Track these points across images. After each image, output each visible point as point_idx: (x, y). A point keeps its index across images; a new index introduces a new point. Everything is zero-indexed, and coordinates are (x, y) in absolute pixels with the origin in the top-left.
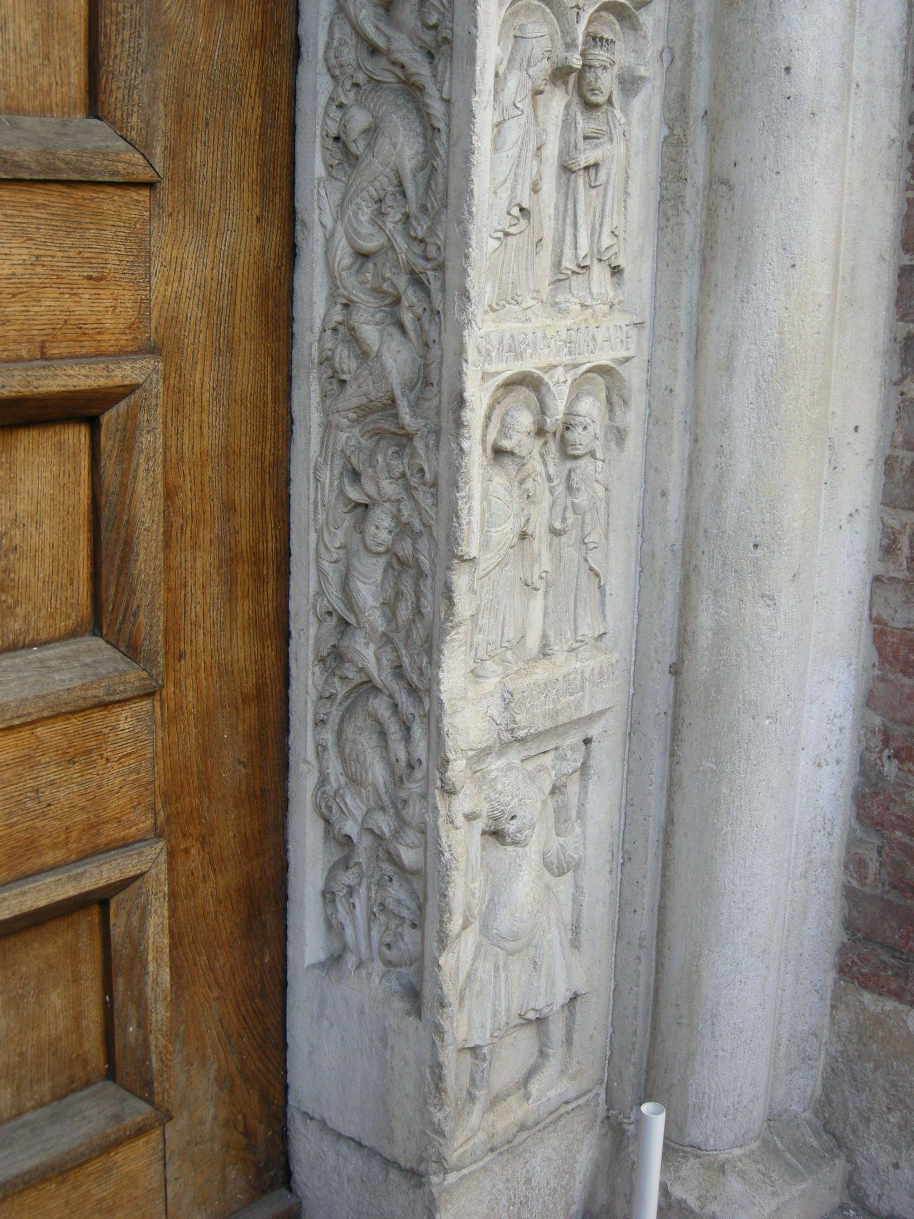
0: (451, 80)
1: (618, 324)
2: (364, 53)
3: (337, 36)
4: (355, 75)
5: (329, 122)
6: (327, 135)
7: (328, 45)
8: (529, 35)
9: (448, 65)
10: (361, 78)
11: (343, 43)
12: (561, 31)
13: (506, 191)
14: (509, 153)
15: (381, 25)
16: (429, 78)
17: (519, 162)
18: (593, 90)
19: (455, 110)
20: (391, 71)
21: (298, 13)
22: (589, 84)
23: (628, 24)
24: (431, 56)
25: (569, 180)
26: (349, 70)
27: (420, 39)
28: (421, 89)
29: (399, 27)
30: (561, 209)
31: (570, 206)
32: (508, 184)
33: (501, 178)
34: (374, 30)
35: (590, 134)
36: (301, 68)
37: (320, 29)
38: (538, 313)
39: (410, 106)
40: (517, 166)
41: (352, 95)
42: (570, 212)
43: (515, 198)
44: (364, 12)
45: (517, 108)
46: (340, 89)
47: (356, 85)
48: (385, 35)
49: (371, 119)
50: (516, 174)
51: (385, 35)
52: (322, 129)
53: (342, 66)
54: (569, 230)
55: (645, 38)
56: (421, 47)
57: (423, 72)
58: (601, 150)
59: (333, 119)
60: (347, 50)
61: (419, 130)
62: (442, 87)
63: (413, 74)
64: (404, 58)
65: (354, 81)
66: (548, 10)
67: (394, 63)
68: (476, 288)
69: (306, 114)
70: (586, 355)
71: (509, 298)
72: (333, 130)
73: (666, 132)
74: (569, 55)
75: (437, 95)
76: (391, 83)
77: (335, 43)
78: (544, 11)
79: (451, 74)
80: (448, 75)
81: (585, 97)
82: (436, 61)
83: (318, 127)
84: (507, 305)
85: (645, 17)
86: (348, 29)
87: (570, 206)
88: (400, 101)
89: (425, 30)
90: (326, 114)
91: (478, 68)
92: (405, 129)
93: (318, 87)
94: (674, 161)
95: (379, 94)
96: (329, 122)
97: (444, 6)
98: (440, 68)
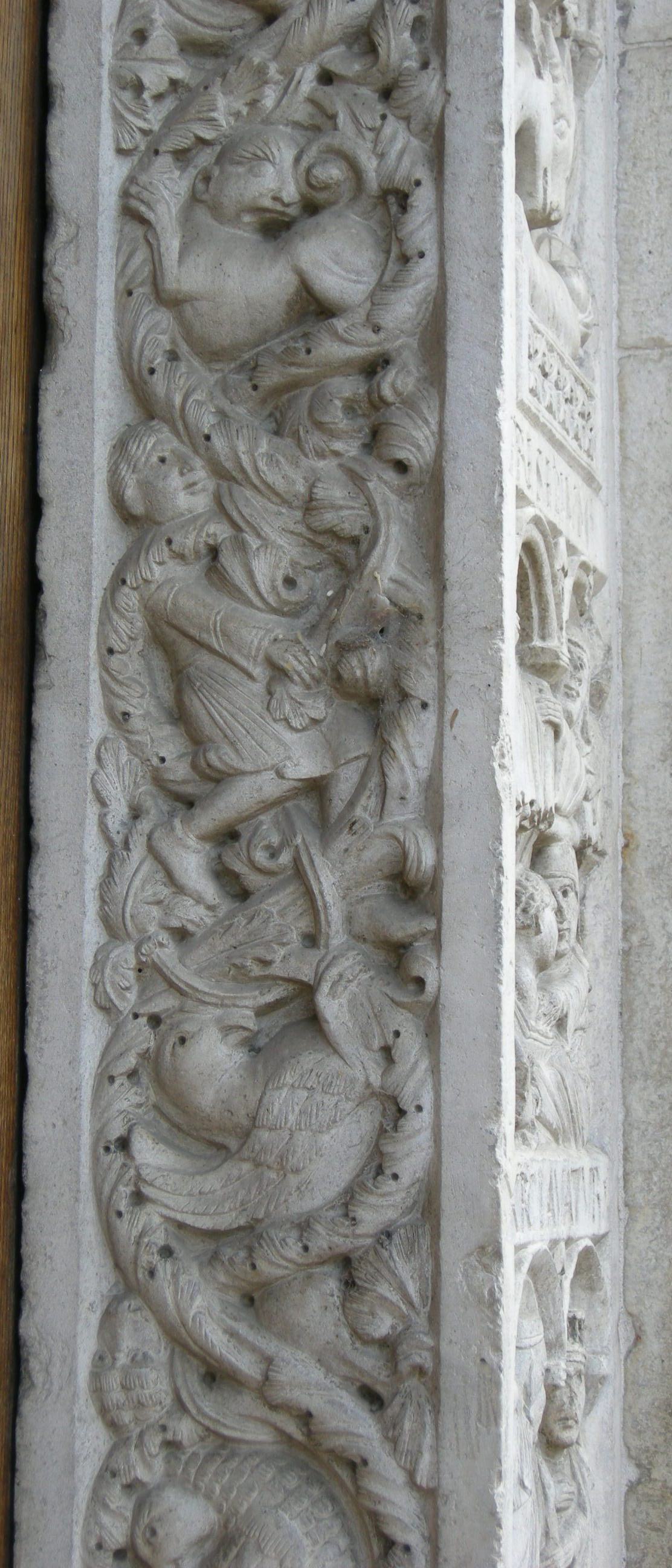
0: (436, 1449)
2: (192, 1385)
3: (127, 1343)
4: (171, 1425)
5: (106, 1519)
6: (100, 1546)
7: (102, 1361)
9: (428, 1419)
10: (185, 1430)
11: (139, 1360)
15: (243, 1329)
16: (376, 1444)
18: (567, 1419)
19: (449, 1511)
20: (265, 1422)
21: (19, 1292)
22: (560, 1409)
23: (584, 1282)
24: (372, 1398)
26: (154, 1414)
27: (345, 1360)
28: (356, 1466)
29: (289, 1335)
34: (225, 1338)
36: (27, 1406)
37: (80, 1326)
39: (316, 1492)
41: (159, 1465)
44: (198, 1301)
46: (134, 1454)
47: (172, 1446)
48: (254, 1349)
49: (213, 1515)
51: (254, 1349)
52: (87, 1533)
53: (140, 1405)
55: (603, 1303)
56: (346, 1378)
57: (361, 1431)
59: (116, 1514)
60: (153, 1375)
61: (343, 1542)
62: (416, 1462)
63: (337, 1433)
64: (314, 1402)
65: (169, 1436)
67: (274, 1407)
69: (44, 1501)
72: (117, 1533)
73: (633, 1473)
74: (552, 1363)
75: (400, 1477)
76: (260, 1443)
77: (123, 1359)
79: (437, 1437)
80: (428, 1440)
81: (551, 1433)
82: (392, 1410)
83: (78, 1530)
86: (152, 1331)
88: (292, 1481)
89: (358, 1345)
90: (97, 1499)
91: (503, 1430)
92: (315, 1543)
93: (78, 1443)
94: (657, 1530)
95: (234, 1464)
96: (106, 1519)
97: (410, 1303)
98: (407, 1425)
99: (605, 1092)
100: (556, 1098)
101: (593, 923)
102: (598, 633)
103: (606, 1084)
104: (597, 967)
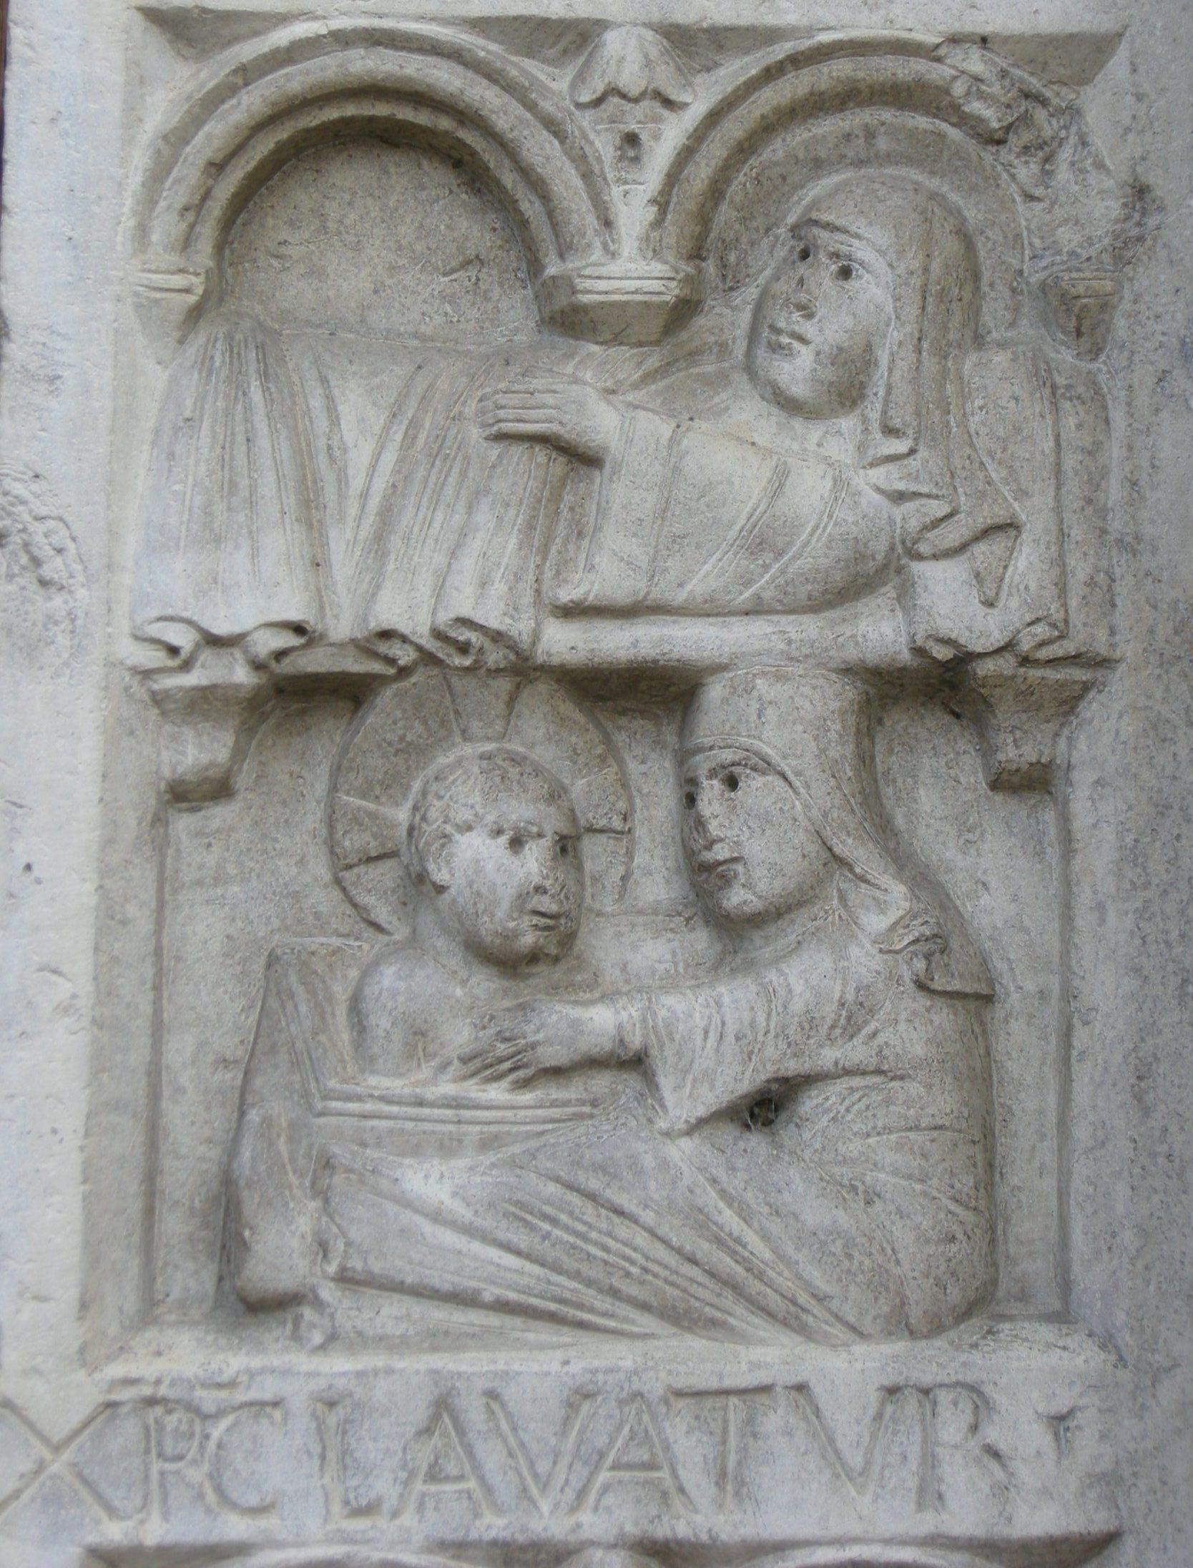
99: (1120, 1209)
100: (521, 1239)
101: (1090, 821)
102: (1100, 166)
103: (1122, 1189)
104: (1102, 921)
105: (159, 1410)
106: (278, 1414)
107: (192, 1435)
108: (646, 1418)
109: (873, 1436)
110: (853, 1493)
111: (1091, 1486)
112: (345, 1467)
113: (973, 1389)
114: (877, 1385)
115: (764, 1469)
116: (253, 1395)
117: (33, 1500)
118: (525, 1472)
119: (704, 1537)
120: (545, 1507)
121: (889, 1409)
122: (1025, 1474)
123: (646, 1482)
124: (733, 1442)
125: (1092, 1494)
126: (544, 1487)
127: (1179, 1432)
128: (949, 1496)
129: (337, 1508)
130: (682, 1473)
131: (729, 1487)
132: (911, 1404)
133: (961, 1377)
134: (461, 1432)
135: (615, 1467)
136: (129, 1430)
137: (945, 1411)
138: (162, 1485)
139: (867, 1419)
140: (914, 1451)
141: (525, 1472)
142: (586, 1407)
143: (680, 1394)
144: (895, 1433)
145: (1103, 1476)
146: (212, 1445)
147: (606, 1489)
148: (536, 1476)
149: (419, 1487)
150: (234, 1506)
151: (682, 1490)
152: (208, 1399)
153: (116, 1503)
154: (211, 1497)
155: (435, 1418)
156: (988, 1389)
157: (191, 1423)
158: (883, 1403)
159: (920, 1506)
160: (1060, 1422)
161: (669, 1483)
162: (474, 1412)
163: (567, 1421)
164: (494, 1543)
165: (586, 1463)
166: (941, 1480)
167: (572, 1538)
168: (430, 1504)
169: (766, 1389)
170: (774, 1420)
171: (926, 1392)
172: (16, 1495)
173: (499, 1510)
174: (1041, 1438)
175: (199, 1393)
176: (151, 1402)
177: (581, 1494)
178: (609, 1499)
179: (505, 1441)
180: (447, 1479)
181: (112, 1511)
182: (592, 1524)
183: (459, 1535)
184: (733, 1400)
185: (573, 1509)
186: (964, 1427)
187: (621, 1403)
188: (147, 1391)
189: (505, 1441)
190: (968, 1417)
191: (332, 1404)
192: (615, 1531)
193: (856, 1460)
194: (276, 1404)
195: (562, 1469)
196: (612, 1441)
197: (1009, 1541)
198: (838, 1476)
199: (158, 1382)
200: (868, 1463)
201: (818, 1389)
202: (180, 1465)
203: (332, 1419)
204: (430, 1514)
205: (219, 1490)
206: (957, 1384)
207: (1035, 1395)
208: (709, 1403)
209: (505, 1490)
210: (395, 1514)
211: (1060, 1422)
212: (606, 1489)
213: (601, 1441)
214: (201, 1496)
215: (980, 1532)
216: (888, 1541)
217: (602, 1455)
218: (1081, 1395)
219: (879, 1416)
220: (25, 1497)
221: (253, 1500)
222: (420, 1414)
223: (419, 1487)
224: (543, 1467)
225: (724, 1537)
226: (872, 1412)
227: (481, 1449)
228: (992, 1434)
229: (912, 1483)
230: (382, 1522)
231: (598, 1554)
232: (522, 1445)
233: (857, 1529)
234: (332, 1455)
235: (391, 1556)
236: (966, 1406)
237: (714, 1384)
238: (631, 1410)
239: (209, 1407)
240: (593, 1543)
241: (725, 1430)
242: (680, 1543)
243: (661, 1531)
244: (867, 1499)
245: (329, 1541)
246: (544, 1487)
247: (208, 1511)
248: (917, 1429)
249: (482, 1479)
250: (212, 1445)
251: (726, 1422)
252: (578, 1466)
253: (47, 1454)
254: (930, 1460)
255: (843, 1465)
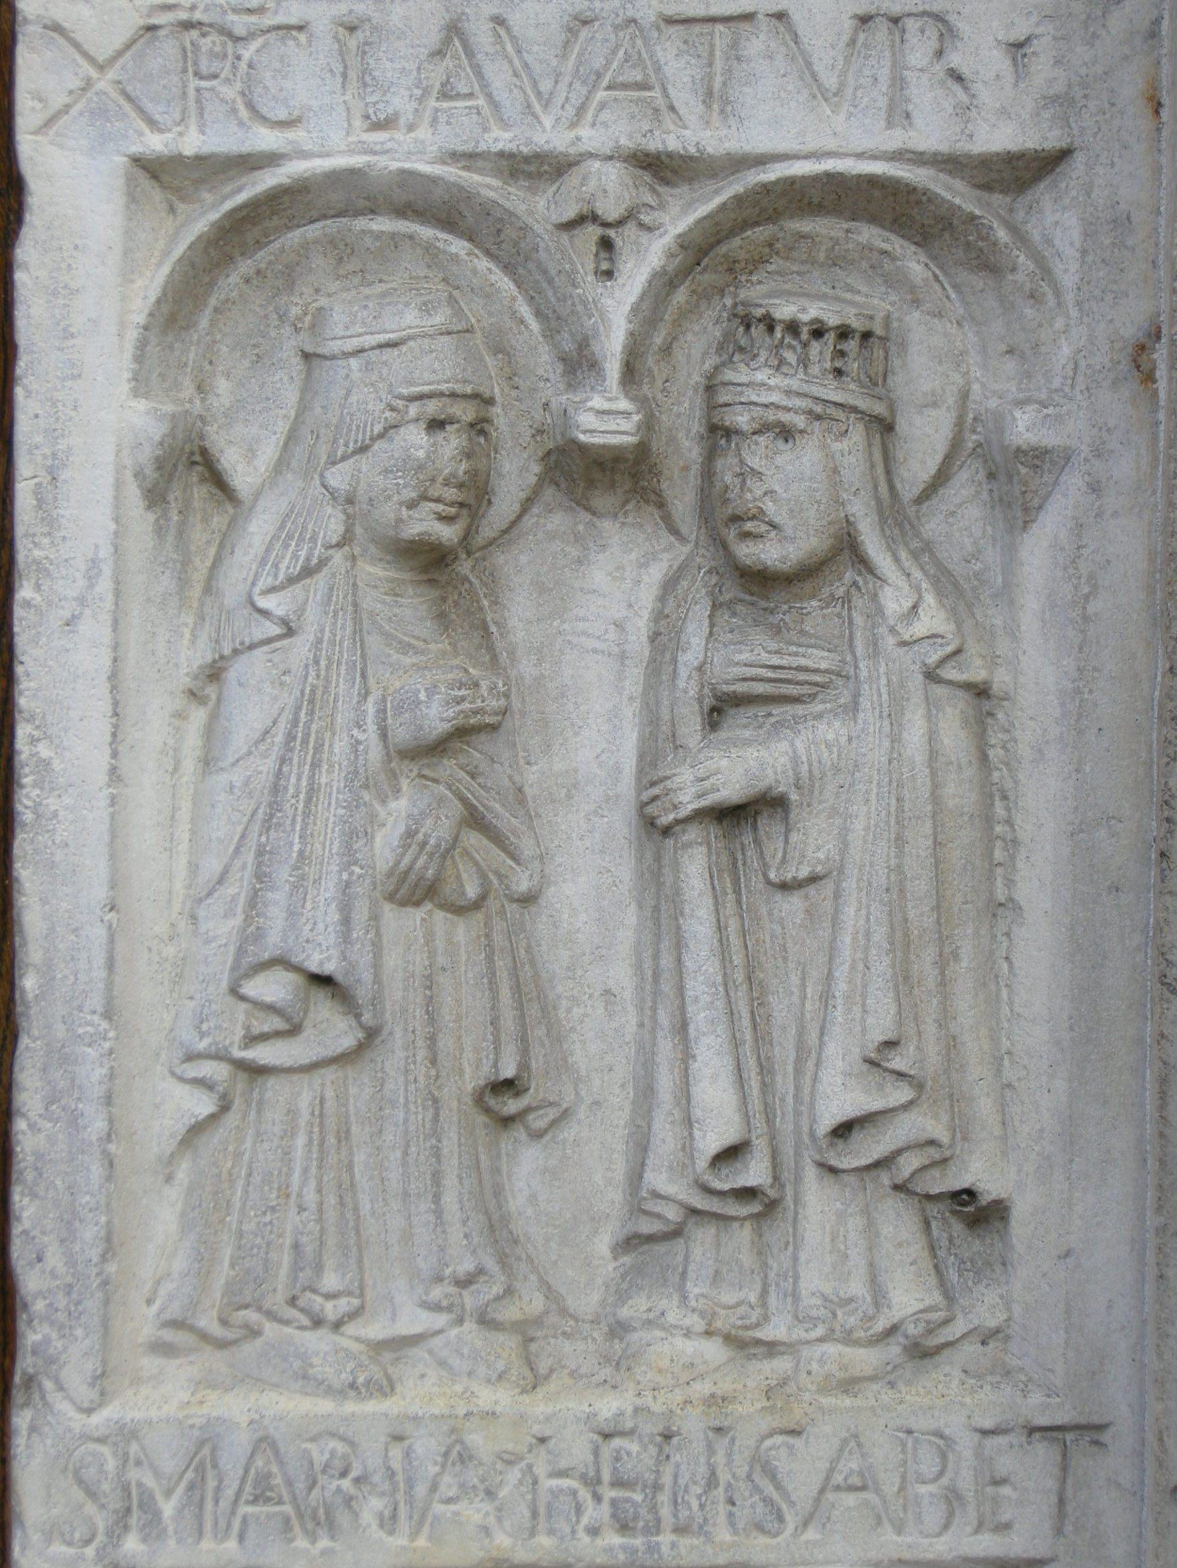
1: (922, 1423)
8: (335, 346)
12: (538, 314)
13: (229, 913)
14: (237, 777)
17: (275, 806)
23: (960, 253)
25: (658, 858)
30: (648, 965)
31: (667, 961)
32: (237, 888)
33: (212, 866)
35: (741, 688)
38: (455, 1362)
40: (268, 825)
42: (667, 987)
43: (259, 936)
45: (264, 613)
50: (261, 852)
54: (666, 1047)
58: (784, 746)
66: (458, 246)
68: (55, 1259)
70: (724, 1535)
71: (277, 1300)
78: (430, 251)
84: (270, 1328)
85: (1050, 217)
87: (667, 961)
105: (194, 33)
106: (303, 37)
107: (225, 55)
108: (639, 42)
109: (848, 59)
110: (829, 112)
111: (1045, 107)
112: (365, 85)
113: (938, 18)
114: (850, 14)
115: (746, 89)
116: (280, 19)
117: (81, 114)
118: (529, 92)
119: (692, 150)
120: (548, 122)
121: (862, 36)
122: (986, 96)
123: (637, 101)
124: (719, 64)
125: (1046, 115)
126: (546, 106)
127: (1126, 58)
128: (915, 114)
129: (358, 123)
130: (671, 91)
131: (715, 106)
132: (881, 30)
133: (927, 7)
134: (470, 53)
135: (609, 88)
136: (168, 49)
137: (912, 38)
138: (198, 101)
139: (842, 45)
140: (884, 74)
141: (529, 92)
142: (584, 33)
143: (670, 21)
144: (866, 57)
145: (1055, 99)
146: (243, 66)
147: (602, 106)
148: (539, 94)
149: (432, 103)
150: (264, 120)
151: (672, 108)
152: (240, 24)
153: (157, 117)
154: (244, 113)
155: (447, 41)
156: (951, 18)
157: (224, 45)
158: (856, 31)
159: (890, 125)
160: (1018, 48)
161: (660, 102)
162: (482, 35)
163: (567, 44)
164: (501, 154)
165: (584, 82)
166: (908, 100)
167: (572, 151)
168: (442, 118)
169: (748, 17)
170: (757, 43)
171: (895, 20)
172: (66, 109)
173: (505, 124)
174: (999, 62)
175: (231, 17)
176: (188, 25)
177: (581, 110)
178: (605, 116)
179: (511, 62)
180: (459, 96)
181: (152, 123)
182: (590, 137)
183: (468, 147)
184: (719, 27)
185: (573, 125)
186: (930, 52)
187: (617, 28)
188: (183, 16)
189: (511, 62)
190: (934, 44)
191: (352, 29)
192: (611, 144)
193: (830, 81)
194: (300, 28)
195: (563, 87)
196: (608, 63)
197: (969, 156)
198: (814, 97)
199: (193, 8)
200: (842, 85)
201: (796, 16)
202: (214, 83)
203: (352, 43)
204: (443, 128)
205: (251, 106)
206: (924, 13)
207: (995, 24)
208: (697, 29)
209: (511, 106)
210: (411, 128)
211: (1018, 48)
212: (602, 106)
213: (598, 62)
214: (234, 111)
215: (944, 148)
216: (860, 156)
217: (599, 75)
218: (1038, 24)
219: (852, 42)
220: (74, 111)
221: (282, 114)
222: (433, 37)
223: (432, 103)
224: (545, 86)
225: (710, 150)
226: (845, 38)
227: (489, 70)
228: (955, 59)
229: (883, 102)
230: (399, 135)
231: (597, 164)
232: (526, 65)
233: (831, 144)
234: (352, 75)
235: (407, 165)
236: (932, 33)
237: (701, 12)
238: (625, 35)
239: (240, 31)
240: (591, 155)
241: (712, 54)
242: (670, 155)
243: (653, 145)
244: (842, 117)
245: (351, 152)
246: (546, 106)
247: (241, 124)
248: (887, 54)
249: (489, 96)
250: (243, 66)
251: (712, 46)
252: (577, 85)
253: (93, 73)
254: (898, 83)
255: (820, 86)
